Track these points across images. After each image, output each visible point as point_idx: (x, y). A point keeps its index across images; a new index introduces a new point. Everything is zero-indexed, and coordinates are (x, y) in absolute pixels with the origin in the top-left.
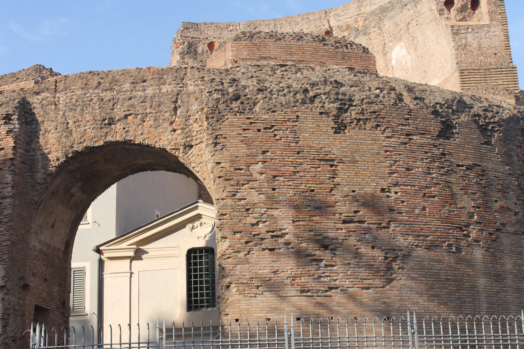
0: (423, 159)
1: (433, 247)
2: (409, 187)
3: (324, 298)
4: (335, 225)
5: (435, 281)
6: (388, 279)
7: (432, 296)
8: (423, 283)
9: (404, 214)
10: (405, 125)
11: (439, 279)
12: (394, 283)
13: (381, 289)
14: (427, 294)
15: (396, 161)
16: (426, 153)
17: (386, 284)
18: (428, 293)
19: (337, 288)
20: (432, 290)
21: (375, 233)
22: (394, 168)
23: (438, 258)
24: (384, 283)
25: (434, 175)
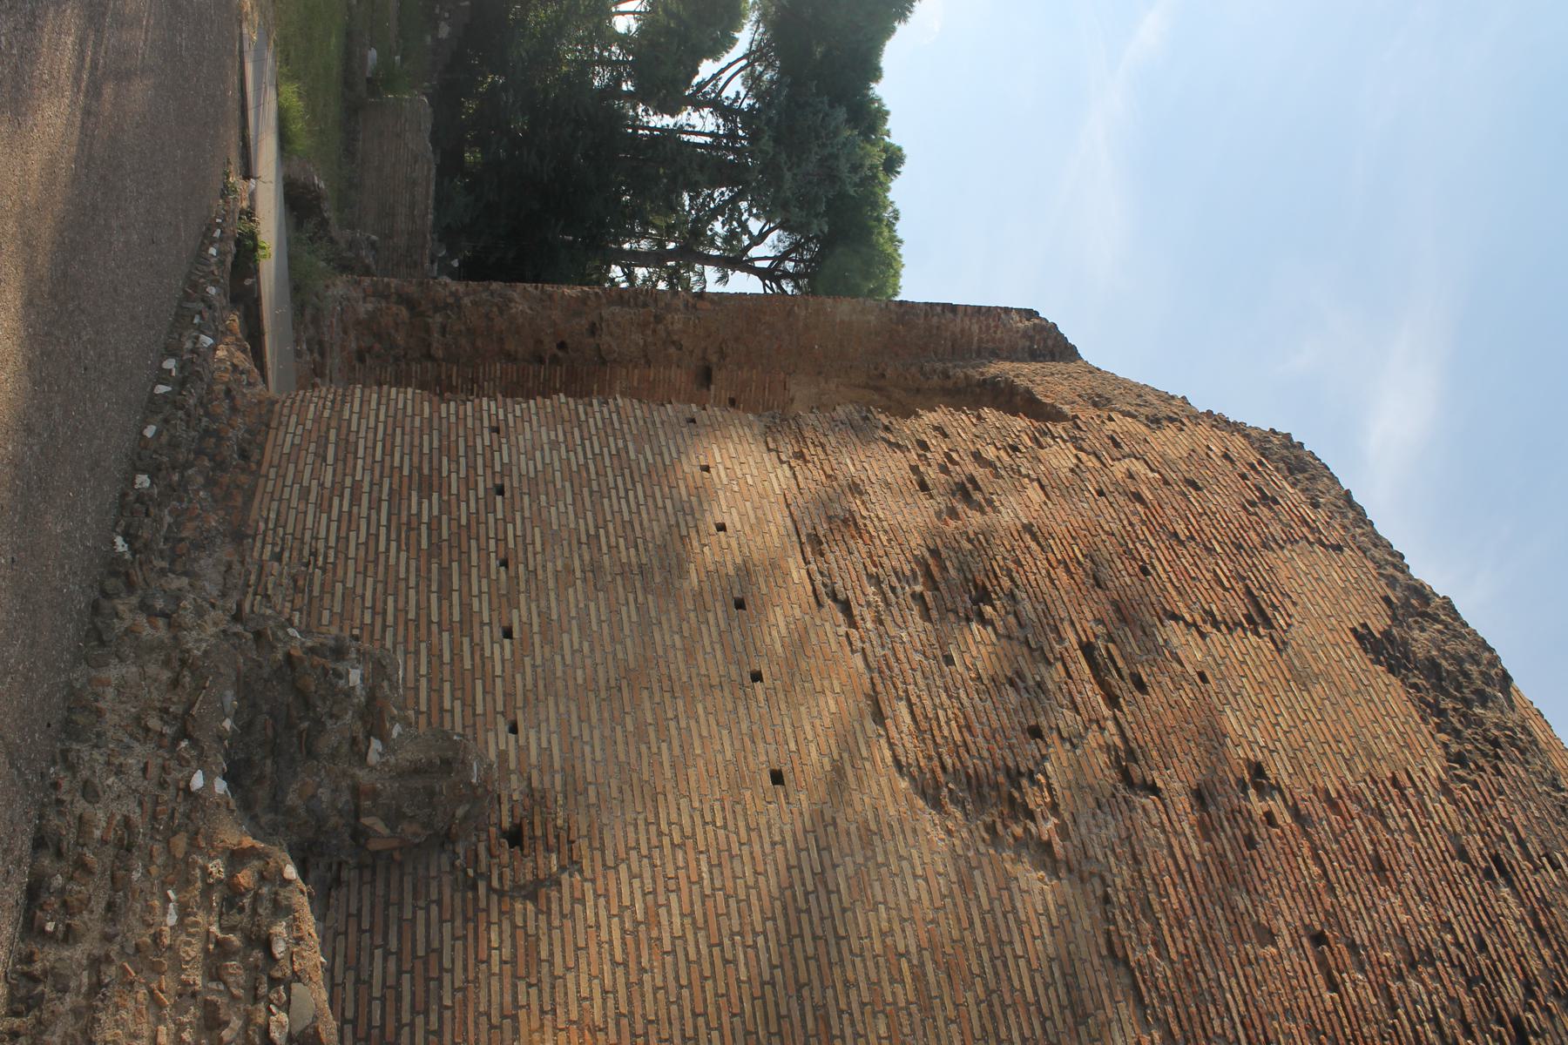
0: (1448, 927)
1: (1127, 981)
2: (1315, 870)
3: (809, 588)
4: (1066, 624)
5: (989, 993)
6: (937, 787)
7: (919, 976)
8: (962, 930)
9: (1206, 844)
10: (1529, 857)
11: (997, 1009)
12: (928, 816)
13: (889, 760)
14: (920, 949)
15: (1382, 817)
16: (1482, 946)
17: (912, 778)
18: (926, 954)
19: (852, 624)
20: (943, 976)
21: (1093, 738)
22: (1355, 809)
23: (1090, 1006)
24: (914, 769)
25: (1413, 984)
